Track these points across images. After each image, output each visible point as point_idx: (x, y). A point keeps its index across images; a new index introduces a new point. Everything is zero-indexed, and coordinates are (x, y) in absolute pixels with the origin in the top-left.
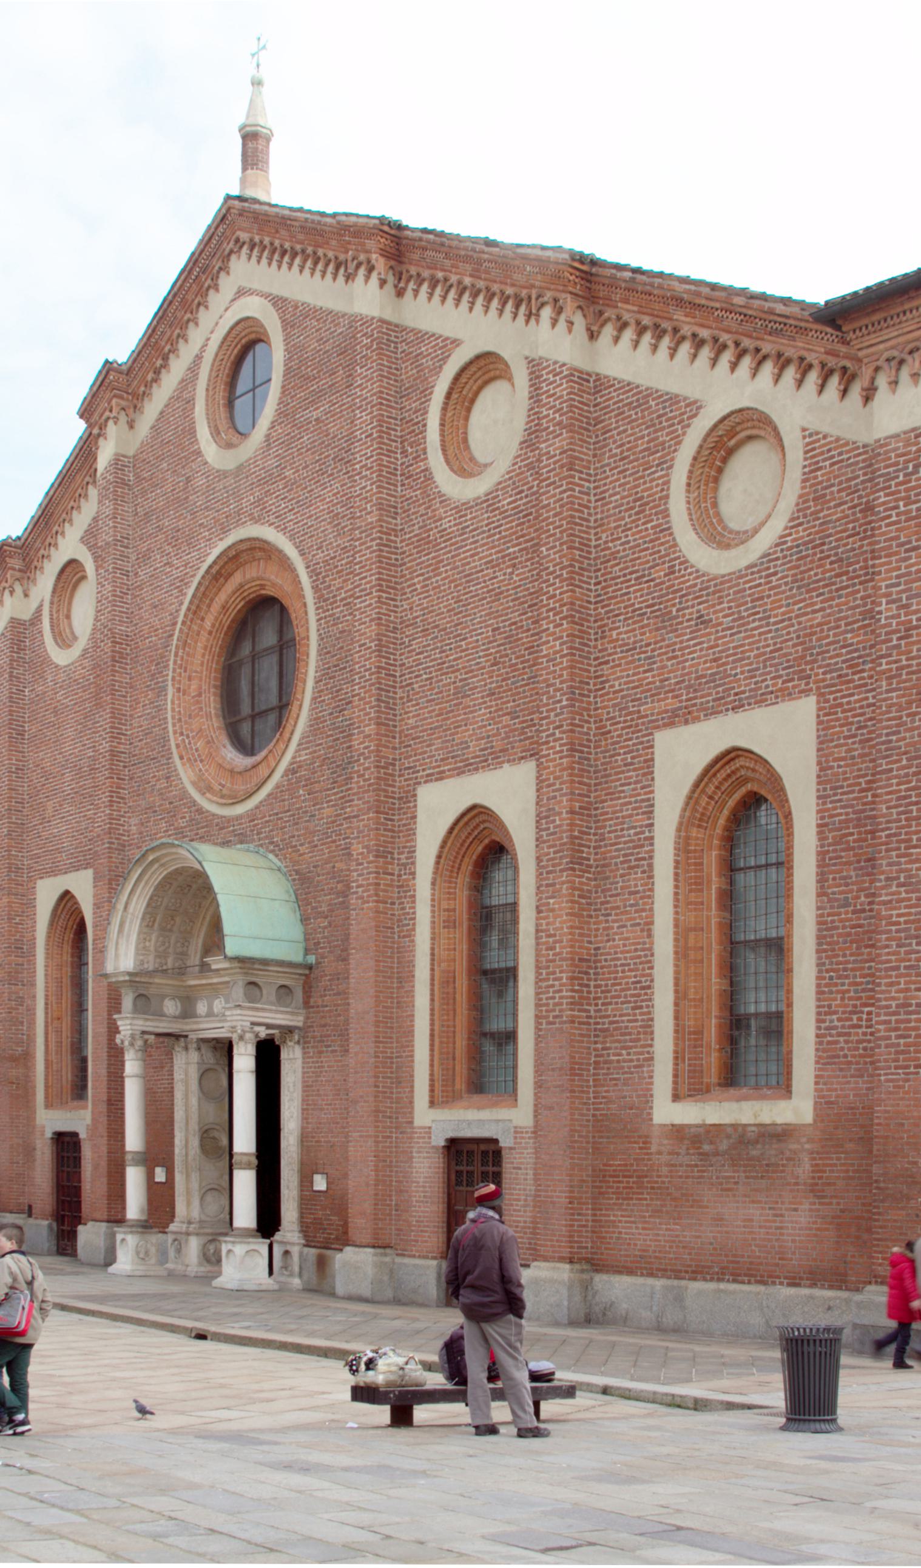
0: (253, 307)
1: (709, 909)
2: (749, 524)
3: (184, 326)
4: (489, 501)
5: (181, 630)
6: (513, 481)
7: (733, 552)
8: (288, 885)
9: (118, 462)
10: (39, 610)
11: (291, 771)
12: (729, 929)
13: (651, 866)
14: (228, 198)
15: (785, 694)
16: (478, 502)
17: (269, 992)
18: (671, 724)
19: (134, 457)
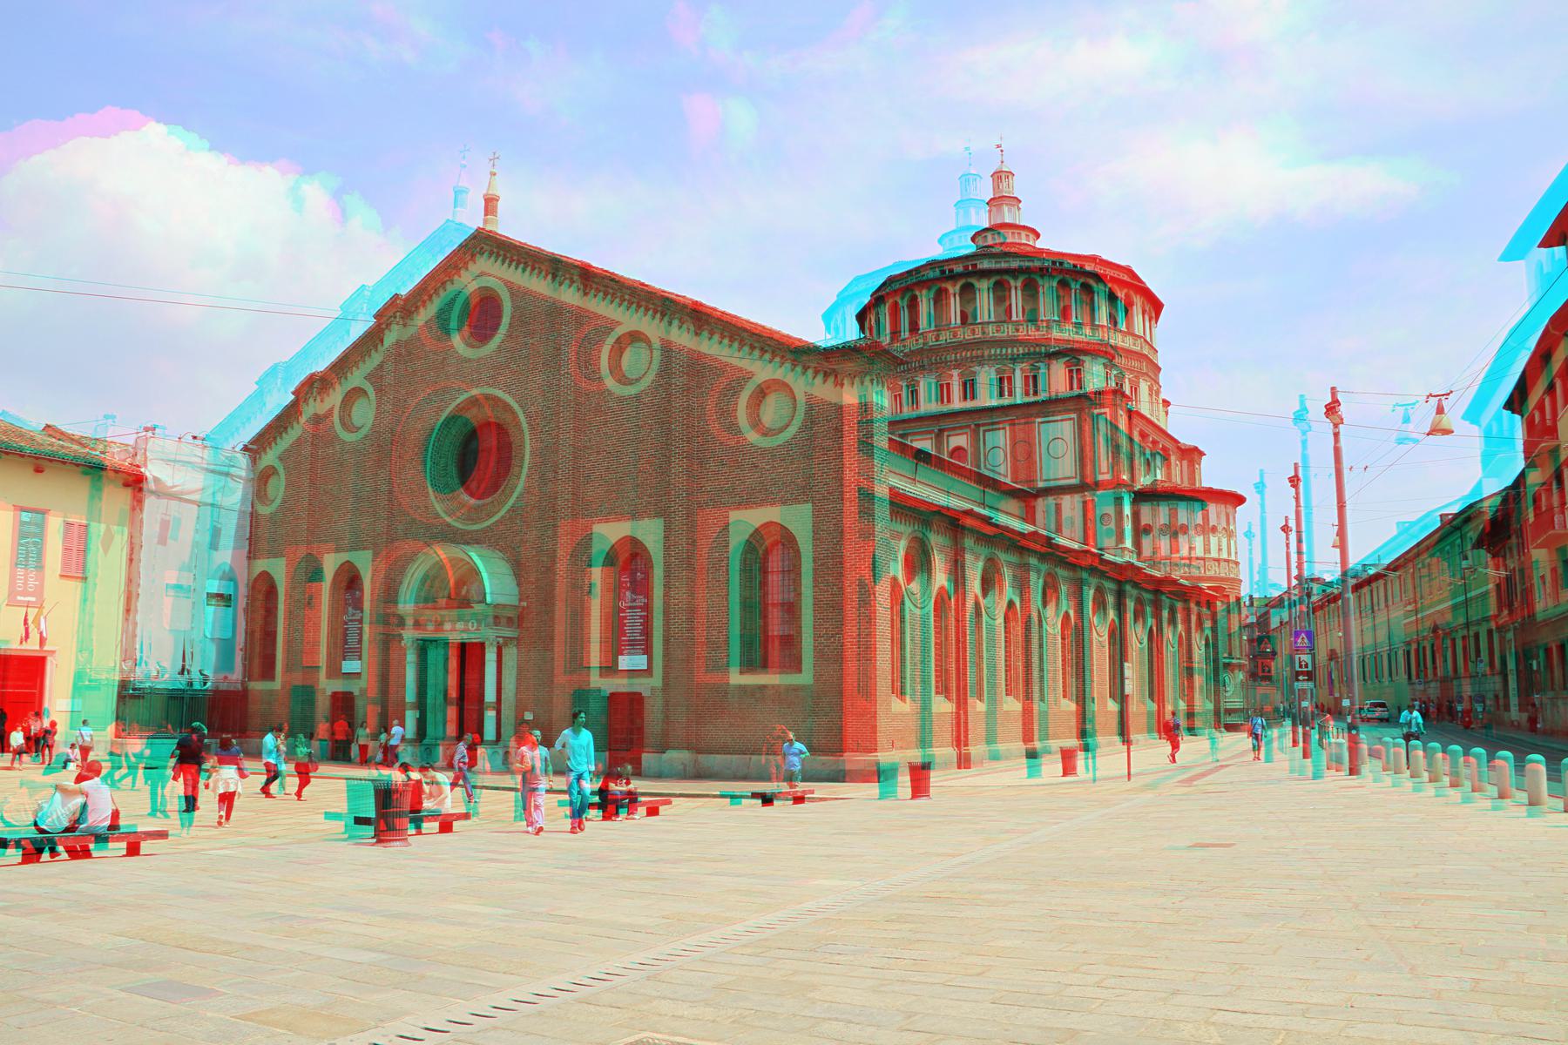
1: (756, 589)
2: (779, 425)
4: (638, 397)
5: (437, 434)
7: (769, 439)
8: (508, 565)
9: (398, 344)
10: (331, 411)
11: (512, 510)
13: (727, 570)
14: (479, 228)
15: (796, 501)
16: (630, 397)
17: (504, 621)
18: (738, 509)
19: (406, 341)
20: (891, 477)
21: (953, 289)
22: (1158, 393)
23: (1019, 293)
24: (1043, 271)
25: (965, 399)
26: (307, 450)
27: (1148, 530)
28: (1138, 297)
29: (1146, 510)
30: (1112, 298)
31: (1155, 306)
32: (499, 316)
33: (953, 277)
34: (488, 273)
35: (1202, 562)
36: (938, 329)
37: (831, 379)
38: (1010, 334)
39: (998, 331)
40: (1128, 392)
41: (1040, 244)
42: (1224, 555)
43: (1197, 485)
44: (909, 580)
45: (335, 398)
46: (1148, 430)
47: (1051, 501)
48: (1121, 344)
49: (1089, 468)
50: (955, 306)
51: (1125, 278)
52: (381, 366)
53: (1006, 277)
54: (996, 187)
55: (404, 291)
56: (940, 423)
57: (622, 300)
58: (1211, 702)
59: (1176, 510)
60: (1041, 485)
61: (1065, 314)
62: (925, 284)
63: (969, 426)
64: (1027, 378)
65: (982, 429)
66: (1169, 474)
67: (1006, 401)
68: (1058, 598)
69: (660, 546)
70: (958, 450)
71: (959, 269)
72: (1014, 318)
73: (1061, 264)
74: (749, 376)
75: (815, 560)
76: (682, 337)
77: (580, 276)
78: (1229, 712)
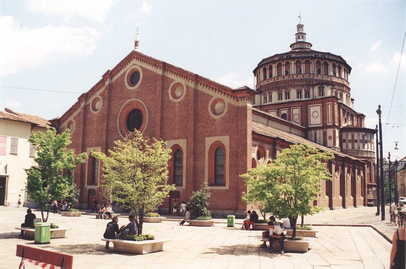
0: (135, 67)
2: (220, 111)
3: (123, 67)
6: (183, 101)
12: (215, 163)
15: (224, 135)
18: (208, 136)
20: (254, 125)
22: (349, 97)
24: (312, 58)
26: (82, 116)
27: (345, 141)
30: (334, 66)
31: (348, 69)
32: (139, 78)
33: (283, 60)
34: (136, 64)
36: (278, 76)
37: (235, 99)
39: (297, 77)
40: (339, 98)
41: (312, 48)
42: (369, 150)
43: (363, 127)
44: (259, 159)
45: (91, 101)
46: (345, 109)
47: (313, 132)
48: (337, 81)
49: (325, 122)
50: (284, 69)
51: (339, 60)
52: (104, 92)
53: (300, 60)
54: (298, 30)
55: (111, 69)
56: (278, 107)
57: (175, 73)
60: (310, 126)
61: (319, 71)
62: (274, 62)
63: (287, 107)
65: (292, 108)
66: (353, 123)
69: (185, 146)
70: (284, 116)
71: (285, 57)
73: (318, 55)
74: (212, 97)
75: (230, 152)
76: (192, 85)
77: (163, 66)
78: (370, 200)
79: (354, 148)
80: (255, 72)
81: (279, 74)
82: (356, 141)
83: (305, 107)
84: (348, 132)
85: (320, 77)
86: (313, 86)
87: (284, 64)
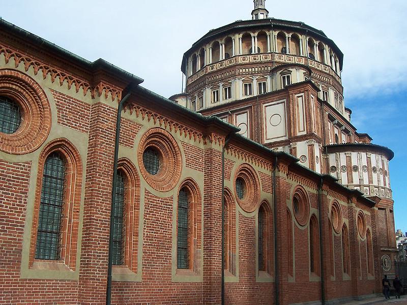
21: (222, 42)
23: (256, 39)
25: (226, 98)
28: (327, 46)
29: (332, 157)
30: (311, 44)
31: (338, 55)
35: (368, 188)
38: (251, 61)
46: (335, 116)
50: (222, 50)
58: (373, 275)
59: (350, 157)
60: (266, 142)
61: (284, 51)
64: (260, 84)
65: (235, 114)
67: (248, 97)
68: (176, 163)
72: (253, 53)
79: (352, 182)
80: (184, 69)
81: (216, 60)
82: (356, 168)
83: (252, 105)
84: (339, 152)
85: (284, 59)
86: (273, 72)
87: (223, 41)
